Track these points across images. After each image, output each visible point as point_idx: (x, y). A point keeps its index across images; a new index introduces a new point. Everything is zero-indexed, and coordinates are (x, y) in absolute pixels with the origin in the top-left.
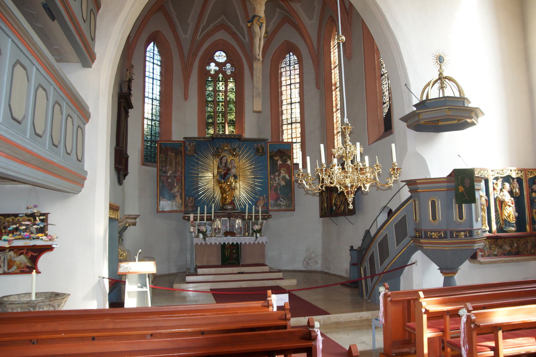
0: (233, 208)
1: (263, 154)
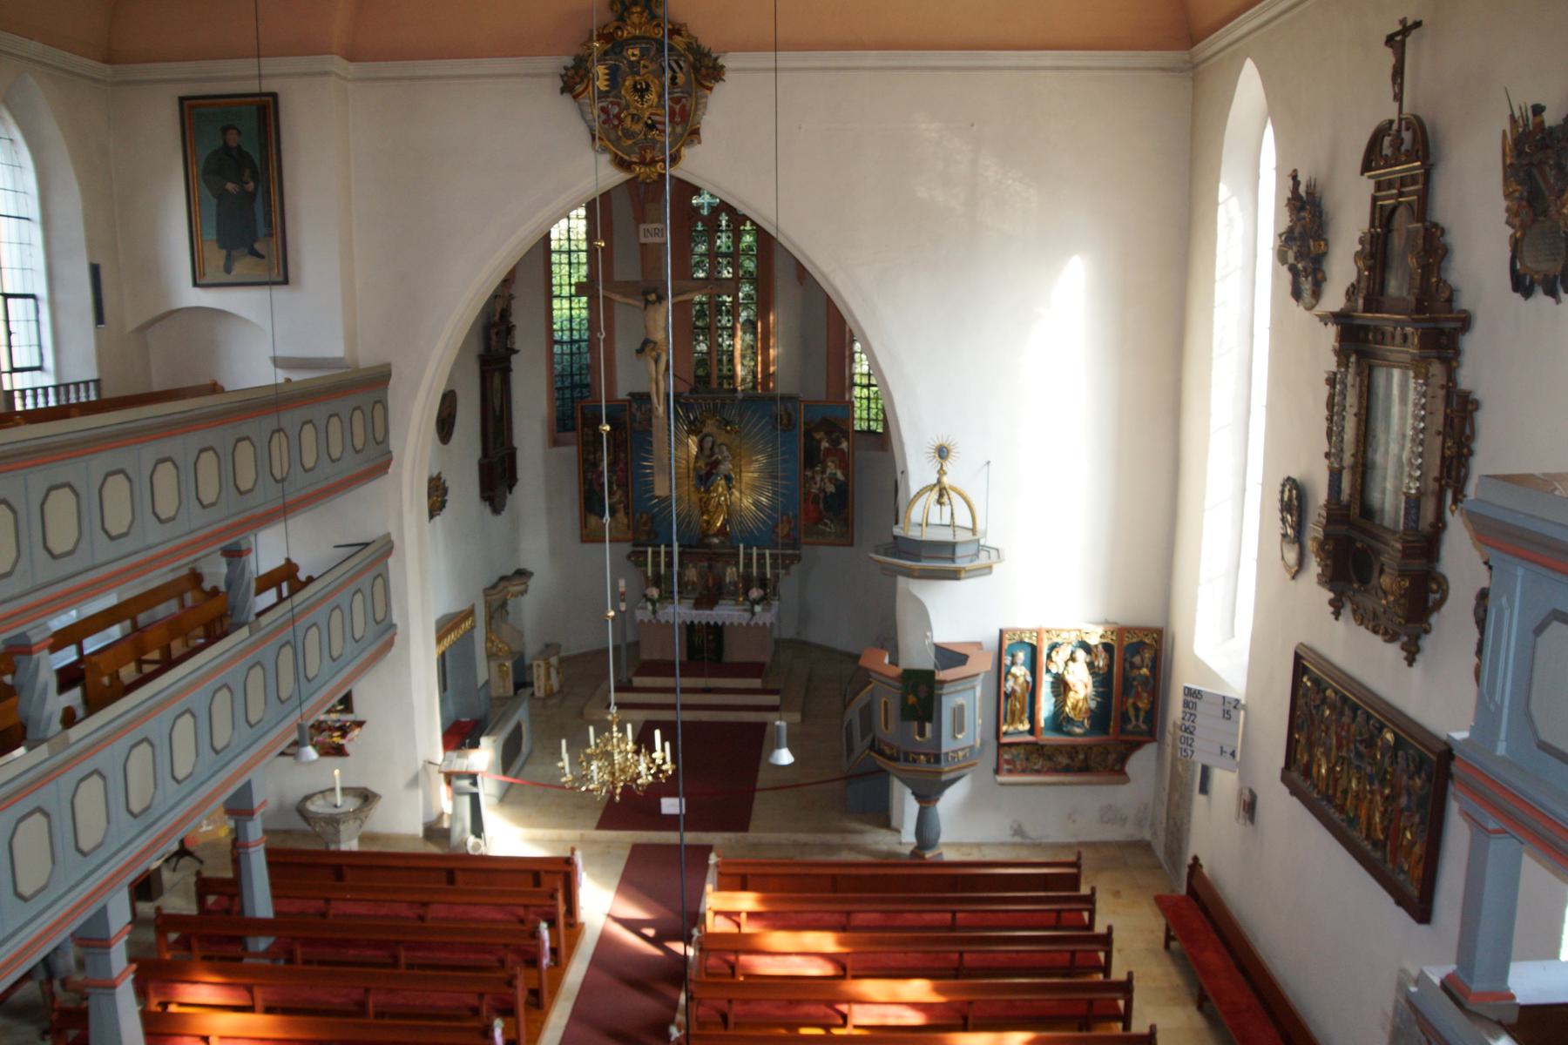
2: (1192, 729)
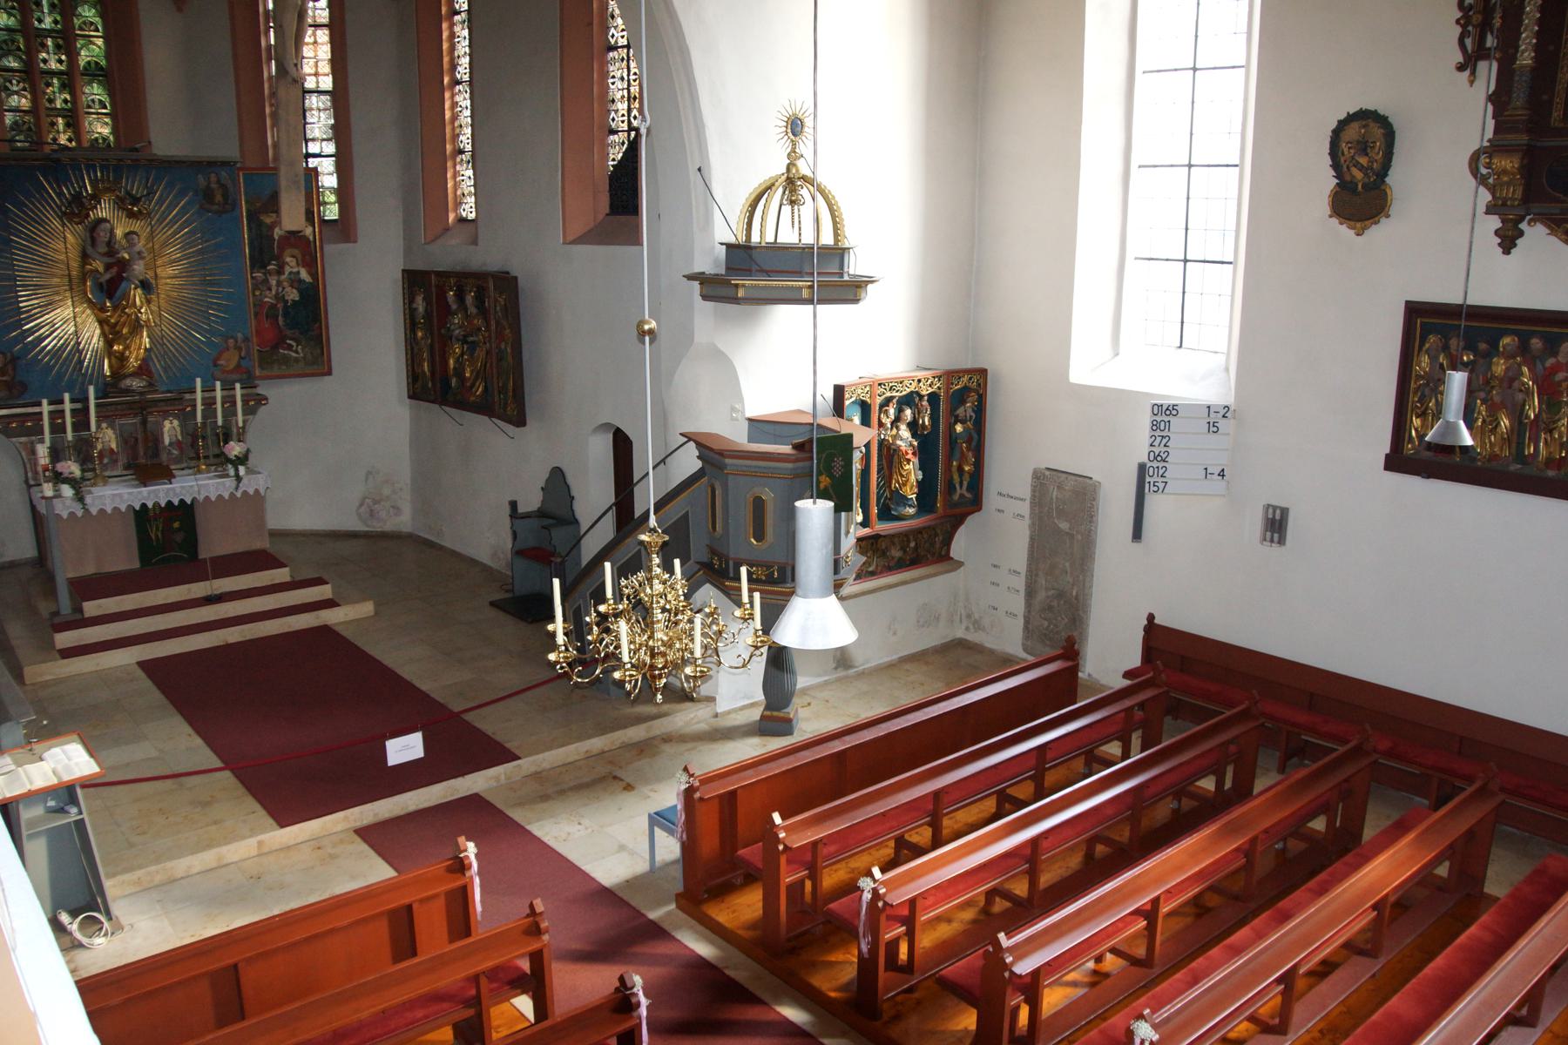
0: (151, 385)
1: (227, 206)
2: (1164, 456)
